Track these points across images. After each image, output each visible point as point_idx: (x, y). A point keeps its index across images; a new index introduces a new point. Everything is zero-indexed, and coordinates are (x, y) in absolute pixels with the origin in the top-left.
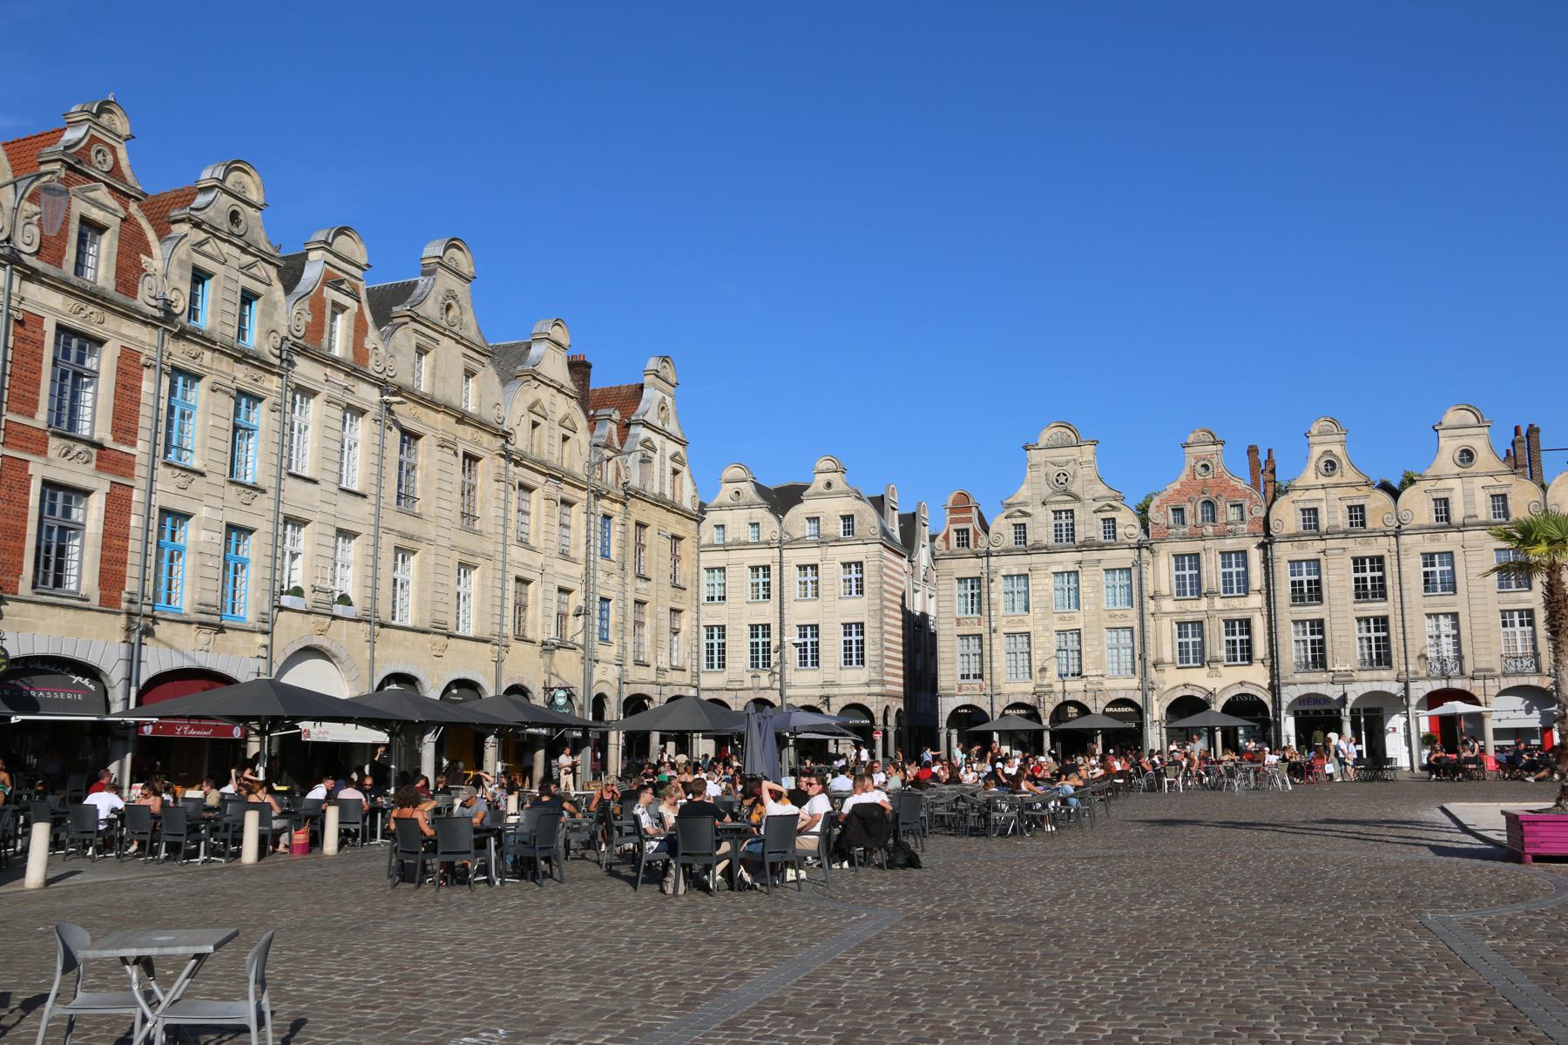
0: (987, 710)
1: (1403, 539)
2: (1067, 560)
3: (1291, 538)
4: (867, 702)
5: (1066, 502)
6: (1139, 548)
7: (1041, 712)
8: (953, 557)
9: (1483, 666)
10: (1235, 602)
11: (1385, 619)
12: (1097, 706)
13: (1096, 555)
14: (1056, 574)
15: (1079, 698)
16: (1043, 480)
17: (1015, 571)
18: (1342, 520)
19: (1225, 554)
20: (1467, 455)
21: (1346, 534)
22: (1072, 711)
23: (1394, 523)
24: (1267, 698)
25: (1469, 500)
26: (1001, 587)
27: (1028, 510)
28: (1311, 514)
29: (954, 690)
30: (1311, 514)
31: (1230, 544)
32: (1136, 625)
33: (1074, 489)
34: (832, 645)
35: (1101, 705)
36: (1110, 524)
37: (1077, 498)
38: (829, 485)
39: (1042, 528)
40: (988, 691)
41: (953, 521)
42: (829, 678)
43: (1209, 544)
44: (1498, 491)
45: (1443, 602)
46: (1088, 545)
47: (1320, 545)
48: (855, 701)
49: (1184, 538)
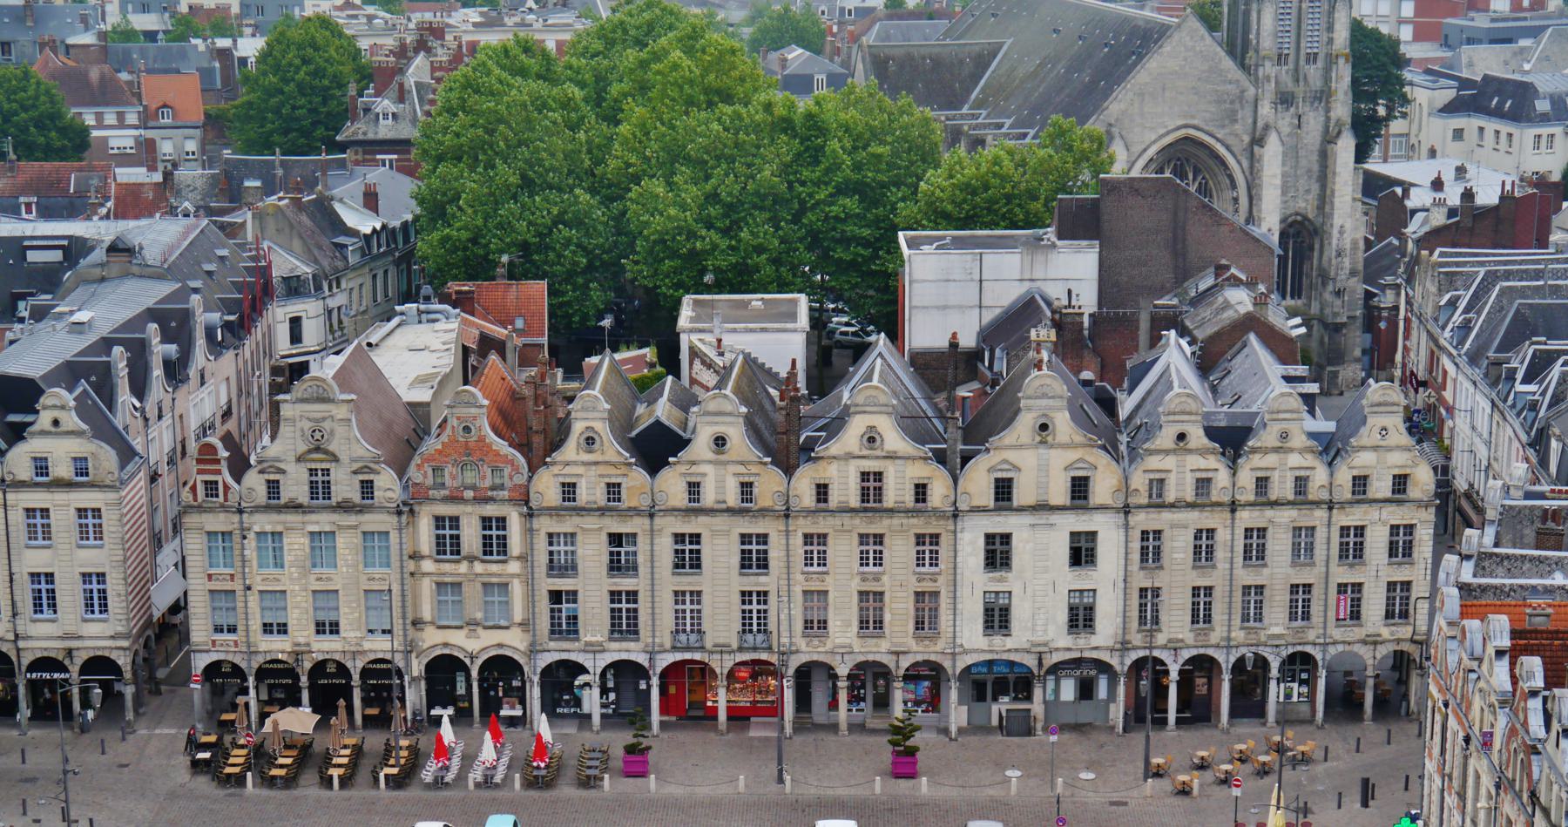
0: (243, 665)
1: (658, 521)
2: (322, 521)
3: (552, 511)
4: (113, 656)
5: (322, 461)
6: (399, 513)
7: (299, 670)
8: (200, 509)
9: (721, 641)
10: (494, 568)
11: (635, 593)
12: (356, 667)
13: (352, 519)
14: (312, 533)
15: (337, 657)
16: (298, 434)
17: (268, 528)
18: (600, 497)
19: (486, 522)
20: (720, 441)
21: (603, 511)
22: (331, 668)
23: (649, 502)
24: (521, 660)
25: (721, 485)
26: (254, 544)
27: (282, 466)
28: (569, 489)
29: (205, 644)
30: (569, 489)
31: (491, 510)
32: (396, 588)
33: (331, 448)
34: (69, 594)
35: (360, 664)
36: (367, 488)
37: (335, 459)
38: (56, 423)
39: (295, 486)
40: (244, 649)
41: (200, 472)
42: (71, 629)
43: (469, 509)
44: (746, 479)
45: (687, 582)
46: (345, 507)
47: (576, 520)
48: (99, 653)
49: (445, 500)
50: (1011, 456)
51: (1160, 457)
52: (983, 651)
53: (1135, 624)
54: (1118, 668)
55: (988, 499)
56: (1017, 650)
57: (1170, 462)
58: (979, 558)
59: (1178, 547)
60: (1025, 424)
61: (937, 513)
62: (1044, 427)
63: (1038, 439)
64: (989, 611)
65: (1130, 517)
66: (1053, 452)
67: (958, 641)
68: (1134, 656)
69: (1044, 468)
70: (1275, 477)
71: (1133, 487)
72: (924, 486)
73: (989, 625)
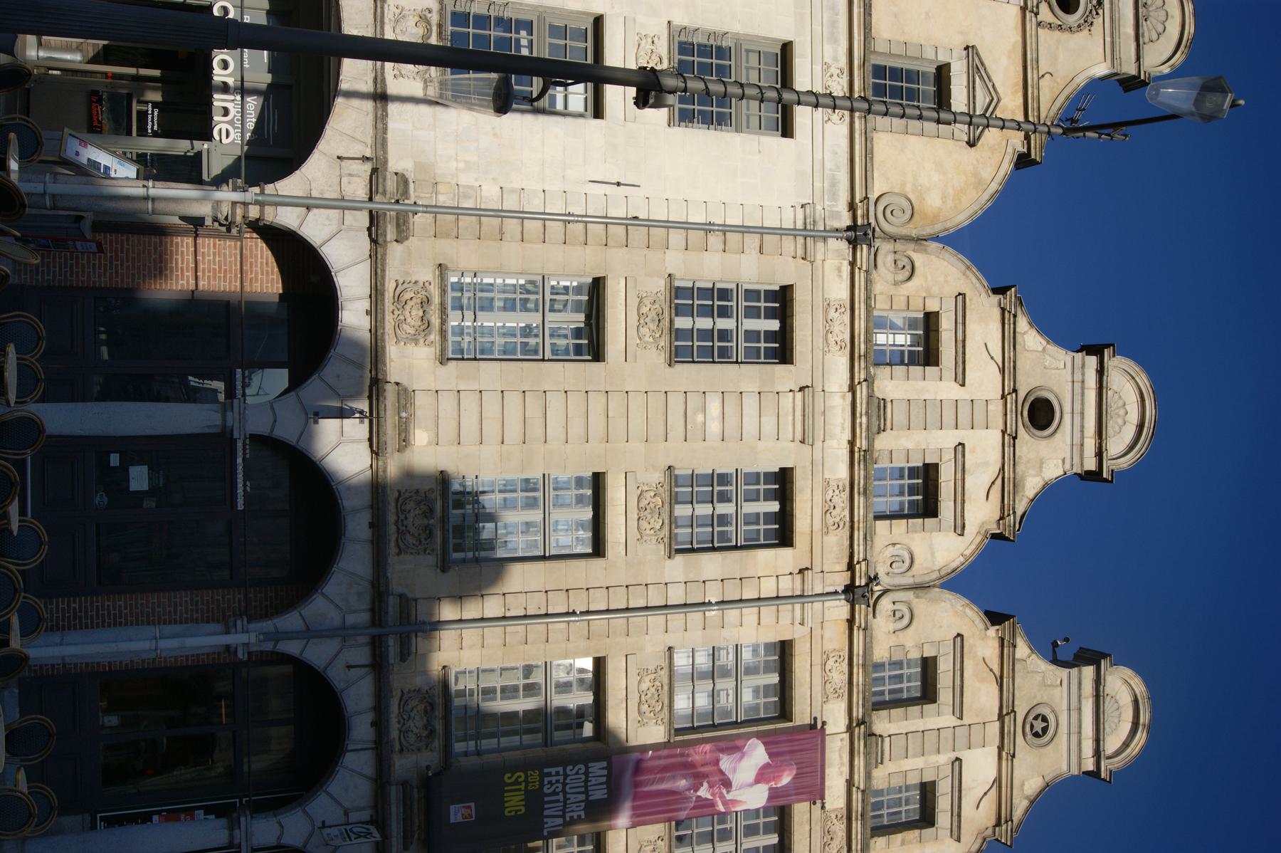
54: (288, 186)
57: (984, 380)
59: (740, 420)
70: (938, 718)
71: (918, 259)
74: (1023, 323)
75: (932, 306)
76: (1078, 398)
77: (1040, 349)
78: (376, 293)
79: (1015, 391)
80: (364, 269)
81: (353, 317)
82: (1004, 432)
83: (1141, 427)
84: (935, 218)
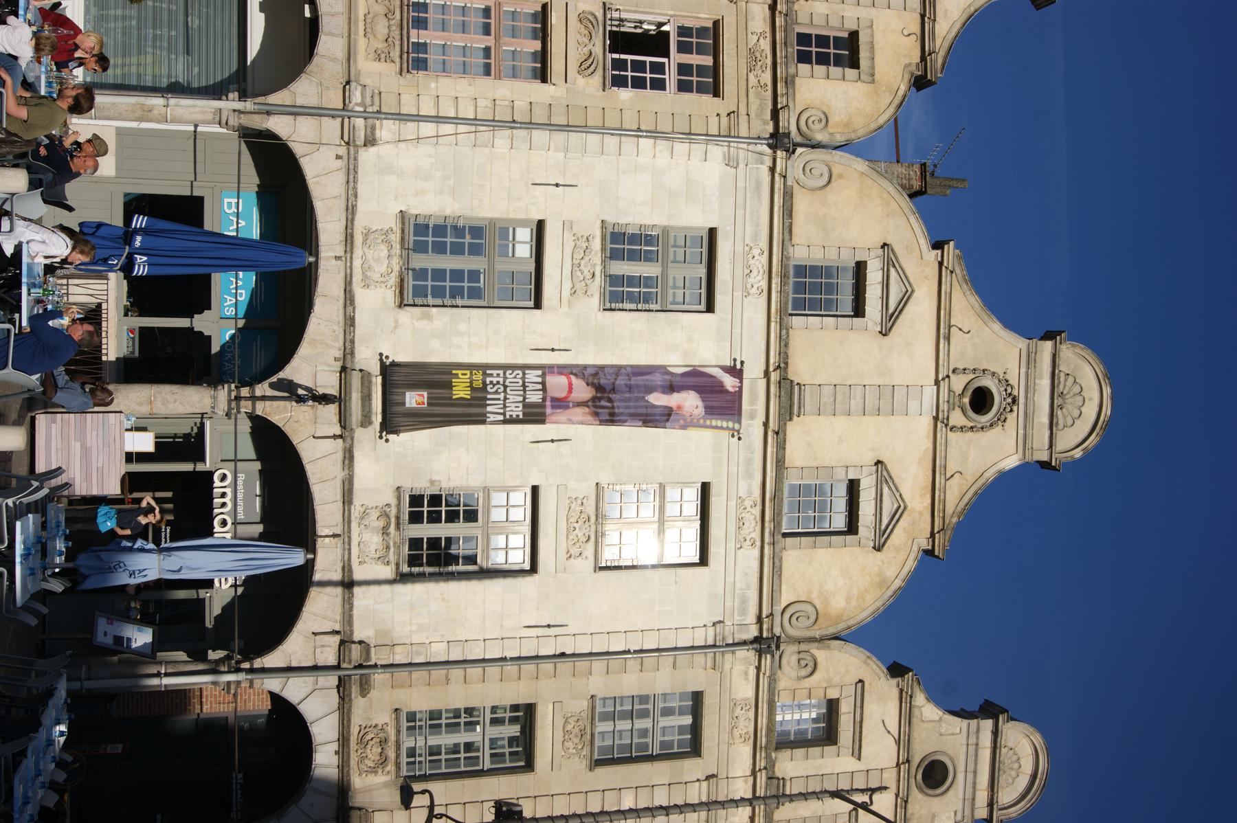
50: (922, 308)
51: (893, 725)
52: (351, 211)
53: (420, 699)
55: (809, 246)
56: (350, 322)
57: (880, 751)
58: (639, 213)
60: (992, 348)
61: (781, 87)
62: (981, 400)
63: (958, 383)
64: (471, 237)
65: (748, 655)
66: (926, 421)
67: (386, 130)
68: (317, 705)
69: (885, 400)
72: (854, 63)
73: (424, 235)
74: (920, 699)
75: (833, 694)
76: (971, 759)
77: (937, 718)
78: (344, 739)
79: (908, 761)
80: (334, 719)
81: (325, 761)
82: (897, 795)
83: (1034, 777)
84: (839, 617)
